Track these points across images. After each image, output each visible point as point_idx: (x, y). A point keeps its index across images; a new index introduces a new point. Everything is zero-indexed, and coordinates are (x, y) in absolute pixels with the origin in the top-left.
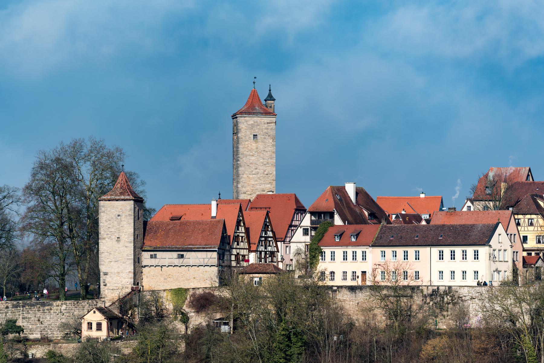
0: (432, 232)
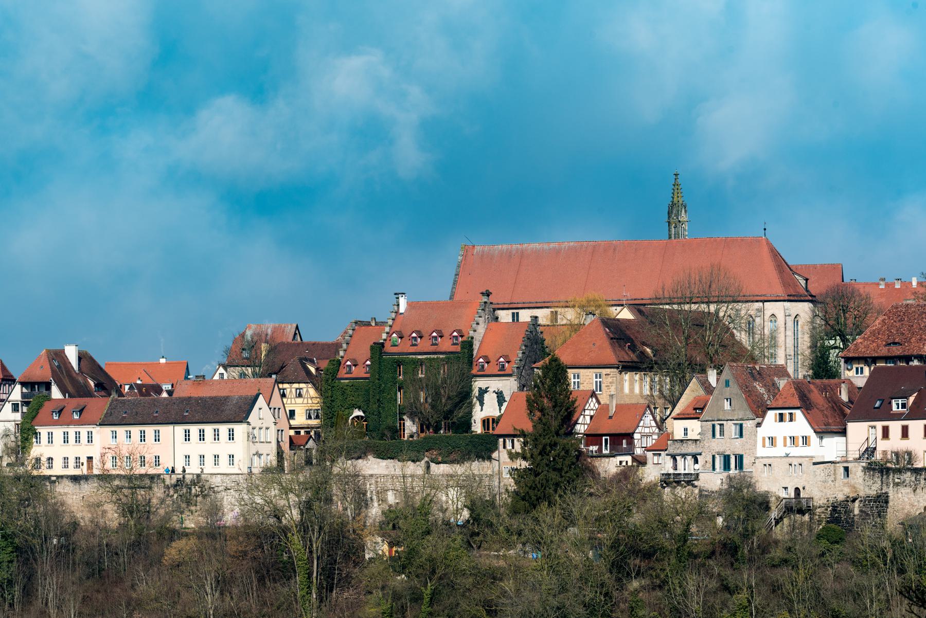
0: (175, 407)
